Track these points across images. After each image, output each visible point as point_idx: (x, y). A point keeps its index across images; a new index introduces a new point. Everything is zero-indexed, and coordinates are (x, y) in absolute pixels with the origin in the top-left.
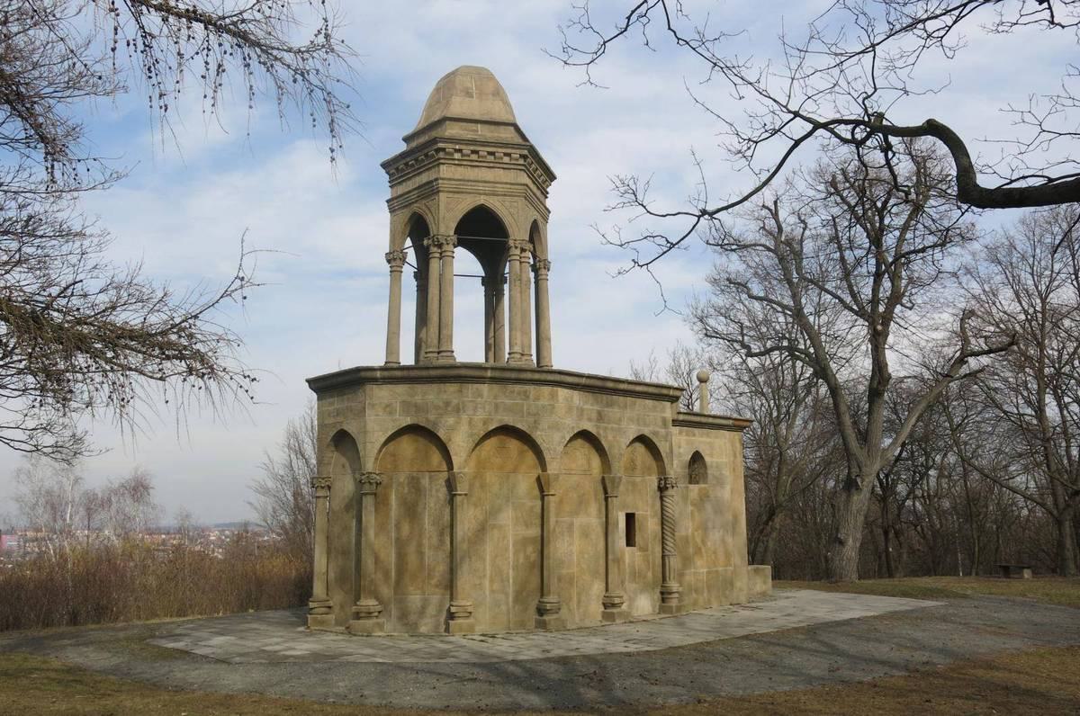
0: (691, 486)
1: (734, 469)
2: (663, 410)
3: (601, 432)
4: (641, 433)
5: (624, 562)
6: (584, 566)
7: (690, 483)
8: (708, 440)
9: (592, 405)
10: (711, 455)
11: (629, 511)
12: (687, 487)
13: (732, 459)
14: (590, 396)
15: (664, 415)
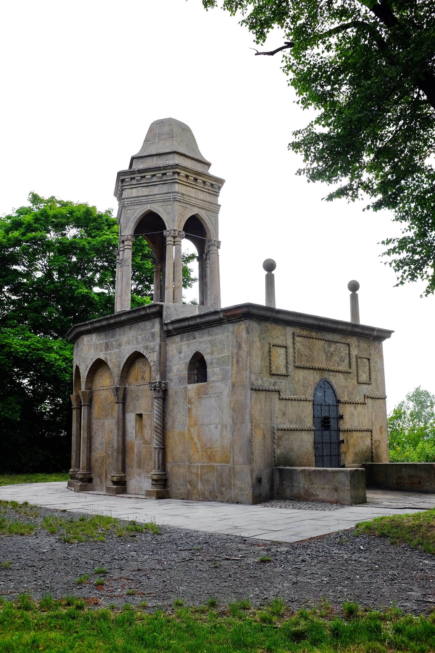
0: (190, 386)
1: (238, 362)
2: (153, 327)
3: (108, 357)
4: (134, 350)
5: (134, 452)
6: (110, 453)
7: (189, 383)
8: (210, 338)
9: (102, 340)
10: (212, 353)
11: (138, 413)
12: (186, 387)
13: (235, 351)
14: (103, 335)
15: (153, 331)
